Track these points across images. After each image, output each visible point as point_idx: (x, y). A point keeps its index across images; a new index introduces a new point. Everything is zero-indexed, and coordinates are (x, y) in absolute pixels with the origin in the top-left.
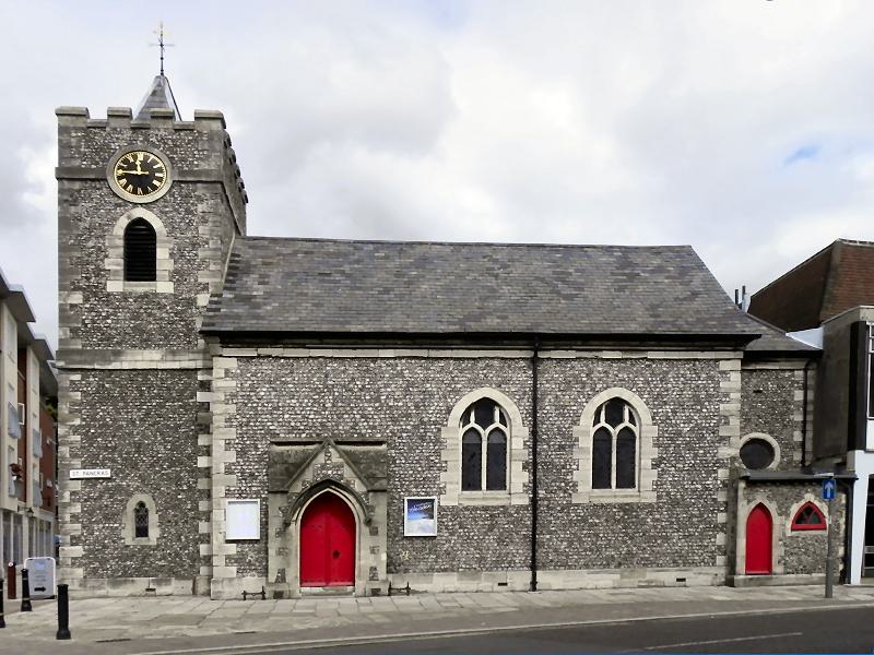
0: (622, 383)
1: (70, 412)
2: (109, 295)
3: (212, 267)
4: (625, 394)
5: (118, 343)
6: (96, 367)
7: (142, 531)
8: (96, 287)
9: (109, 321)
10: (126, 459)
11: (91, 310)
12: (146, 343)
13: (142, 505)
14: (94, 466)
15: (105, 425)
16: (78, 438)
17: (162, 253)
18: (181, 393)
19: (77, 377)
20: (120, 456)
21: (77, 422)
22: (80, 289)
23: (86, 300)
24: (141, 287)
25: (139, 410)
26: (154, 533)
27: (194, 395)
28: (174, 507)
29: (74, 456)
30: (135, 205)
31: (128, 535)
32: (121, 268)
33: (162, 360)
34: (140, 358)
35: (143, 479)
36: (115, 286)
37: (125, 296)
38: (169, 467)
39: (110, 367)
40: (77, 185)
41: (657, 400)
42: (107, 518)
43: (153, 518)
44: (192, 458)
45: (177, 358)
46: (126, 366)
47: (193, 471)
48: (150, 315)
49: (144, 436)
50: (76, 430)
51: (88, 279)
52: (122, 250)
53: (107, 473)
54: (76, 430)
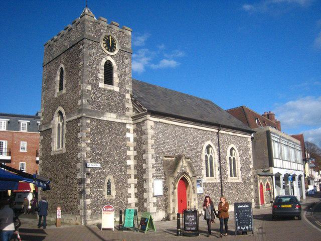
0: (233, 143)
1: (87, 137)
2: (100, 88)
3: (130, 84)
4: (235, 147)
5: (103, 109)
6: (96, 118)
7: (109, 193)
8: (96, 84)
9: (100, 99)
10: (104, 160)
11: (94, 93)
12: (111, 111)
13: (109, 180)
14: (94, 162)
15: (98, 144)
16: (88, 149)
17: (115, 75)
18: (122, 132)
19: (89, 121)
20: (103, 158)
21: (89, 141)
22: (90, 84)
23: (92, 89)
24: (109, 87)
25: (109, 138)
26: (114, 193)
27: (125, 134)
28: (120, 182)
29: (88, 157)
30: (108, 55)
31: (105, 193)
32: (103, 78)
33: (117, 118)
34: (110, 116)
35: (110, 168)
36: (102, 85)
37: (105, 90)
38: (119, 164)
39: (100, 119)
40: (91, 42)
41: (239, 149)
42: (99, 186)
43: (113, 186)
44: (125, 160)
45: (121, 118)
46: (105, 119)
47: (126, 166)
48: (112, 99)
49: (111, 150)
50: (88, 145)
51: (93, 80)
52: (103, 71)
53: (98, 165)
54: (88, 145)
